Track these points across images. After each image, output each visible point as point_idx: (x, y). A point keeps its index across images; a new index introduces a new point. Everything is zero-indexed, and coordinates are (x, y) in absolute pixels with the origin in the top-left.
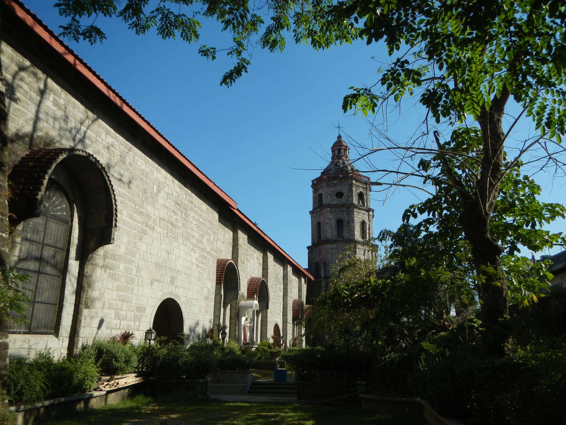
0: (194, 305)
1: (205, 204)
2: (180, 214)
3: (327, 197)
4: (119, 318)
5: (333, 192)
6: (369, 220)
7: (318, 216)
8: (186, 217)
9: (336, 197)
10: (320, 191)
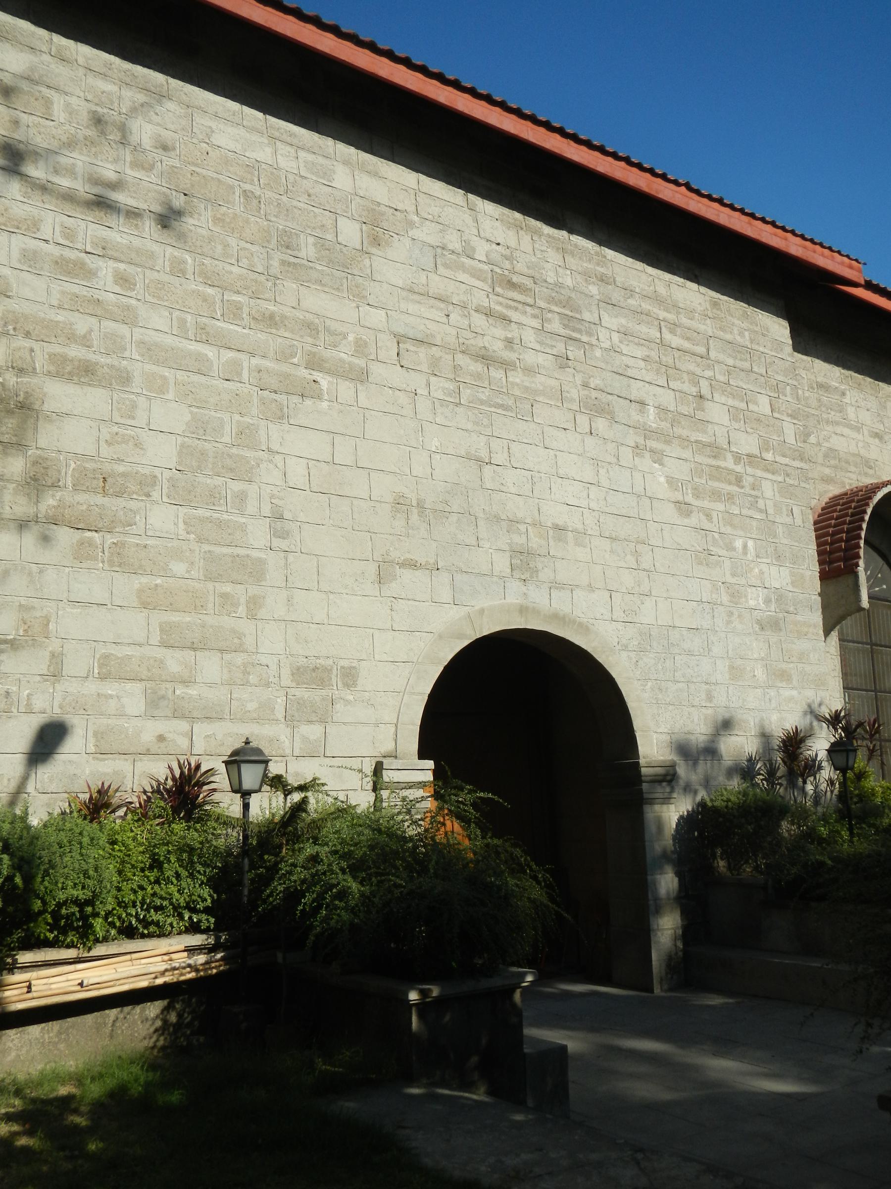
0: (690, 653)
1: (694, 286)
2: (536, 323)
4: (178, 714)
8: (580, 331)
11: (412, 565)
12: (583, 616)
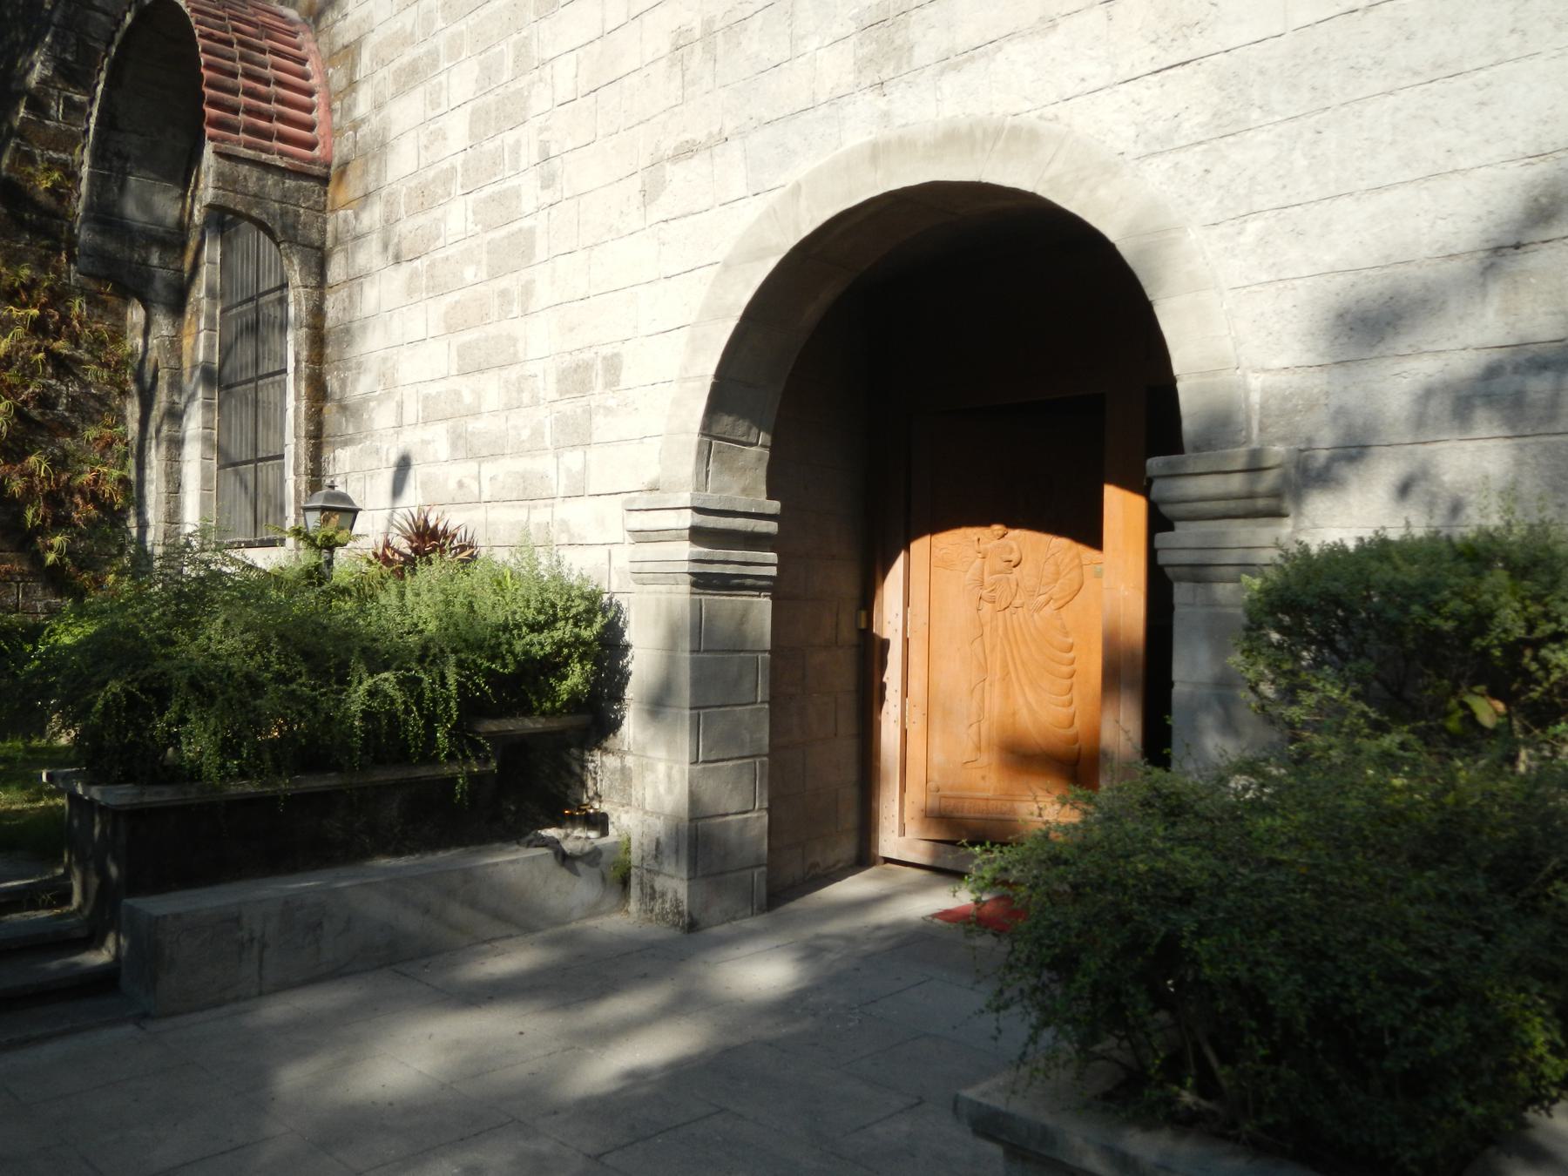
11: (687, 151)
12: (1028, 106)
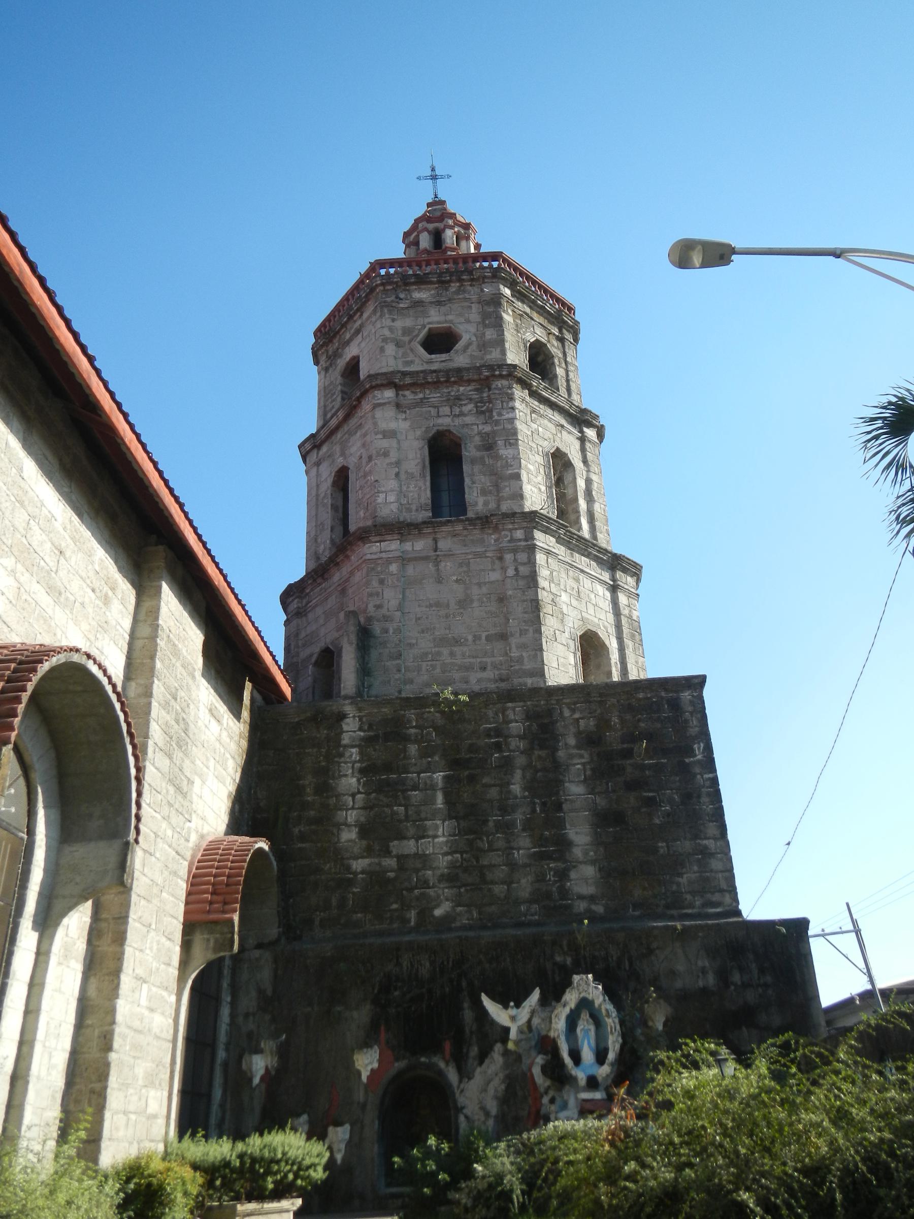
3: (382, 350)
5: (406, 331)
6: (585, 461)
7: (337, 448)
9: (422, 351)
10: (351, 351)
